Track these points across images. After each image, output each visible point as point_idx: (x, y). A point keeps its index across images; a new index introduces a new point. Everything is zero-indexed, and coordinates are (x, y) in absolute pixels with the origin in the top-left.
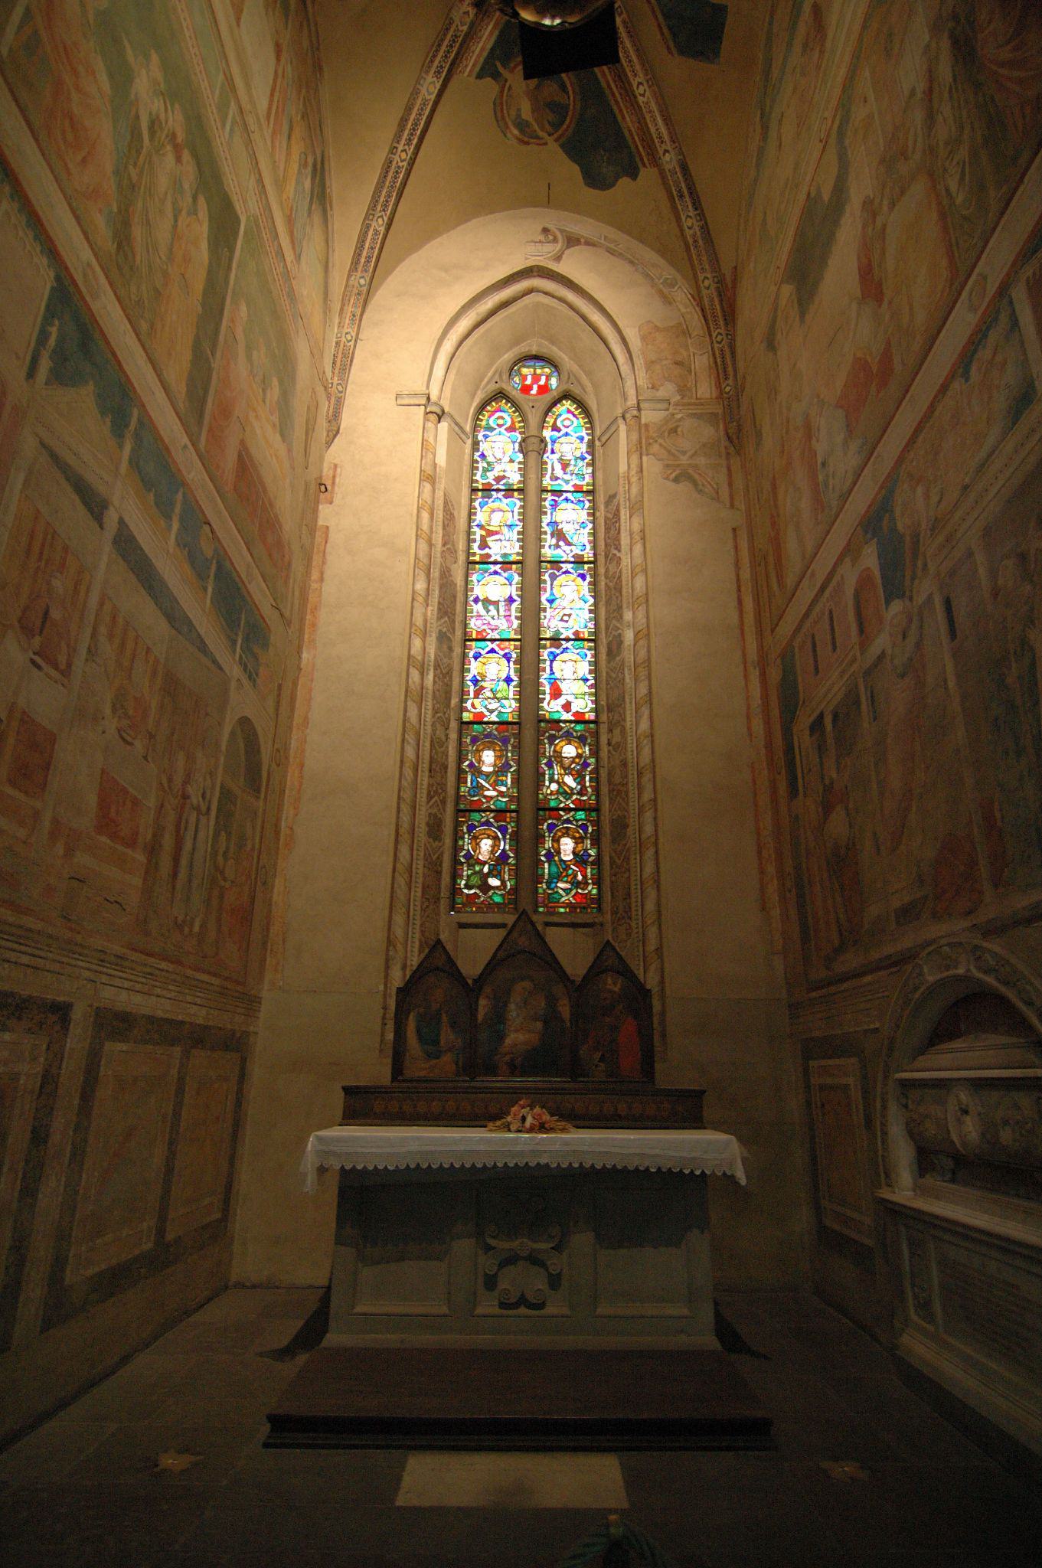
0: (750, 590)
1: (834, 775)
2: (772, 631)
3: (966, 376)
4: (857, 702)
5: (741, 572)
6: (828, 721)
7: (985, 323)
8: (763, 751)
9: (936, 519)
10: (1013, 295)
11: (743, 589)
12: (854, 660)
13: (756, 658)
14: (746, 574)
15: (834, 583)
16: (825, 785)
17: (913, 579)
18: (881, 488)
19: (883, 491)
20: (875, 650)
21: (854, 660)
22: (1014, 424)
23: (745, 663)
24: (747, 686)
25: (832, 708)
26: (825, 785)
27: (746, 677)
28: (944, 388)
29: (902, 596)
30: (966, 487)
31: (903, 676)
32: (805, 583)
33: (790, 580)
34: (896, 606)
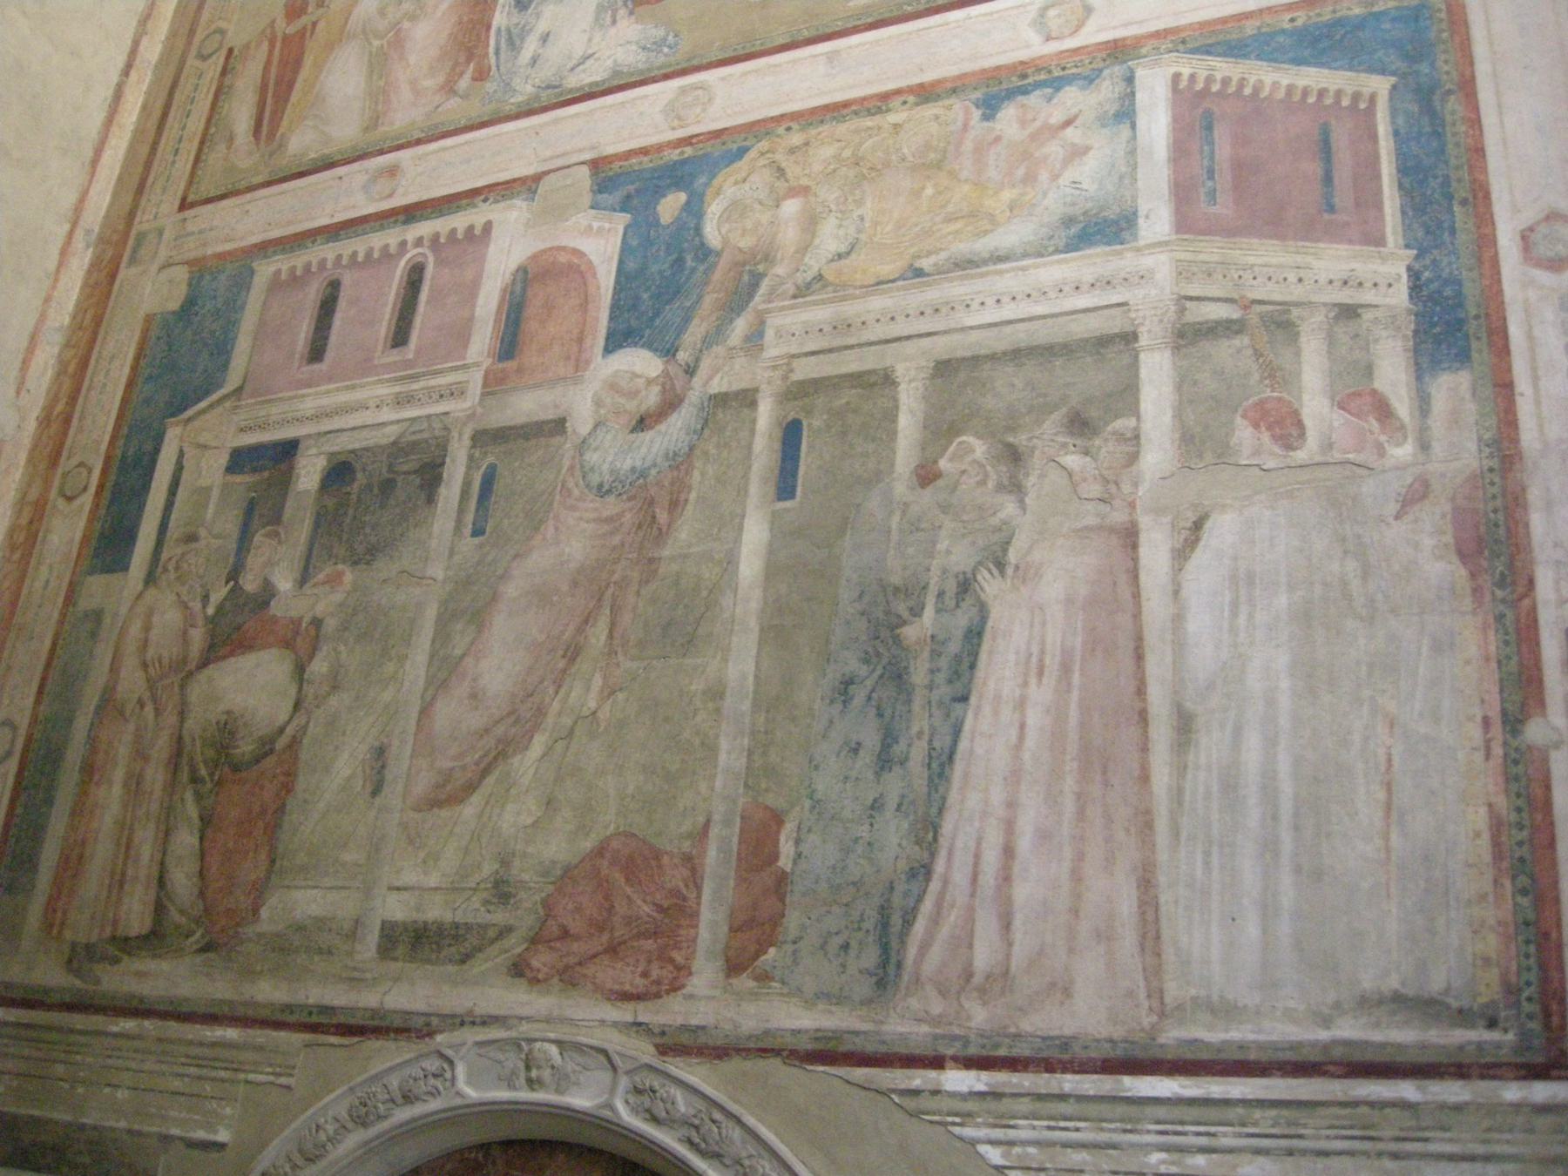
0: (144, 88)
1: (284, 583)
2: (184, 205)
3: (990, 107)
4: (431, 475)
5: (145, 42)
6: (309, 473)
7: (1064, 69)
8: (31, 425)
9: (820, 277)
10: (1140, 73)
11: (134, 75)
12: (456, 392)
13: (97, 228)
14: (152, 51)
15: (458, 221)
16: (236, 590)
17: (708, 342)
18: (687, 141)
19: (689, 151)
20: (526, 406)
21: (456, 392)
22: (1070, 248)
23: (74, 224)
24: (58, 270)
25: (336, 449)
26: (236, 590)
27: (64, 253)
28: (925, 93)
29: (669, 353)
30: (919, 273)
31: (602, 491)
32: (356, 173)
33: (301, 142)
34: (641, 363)
